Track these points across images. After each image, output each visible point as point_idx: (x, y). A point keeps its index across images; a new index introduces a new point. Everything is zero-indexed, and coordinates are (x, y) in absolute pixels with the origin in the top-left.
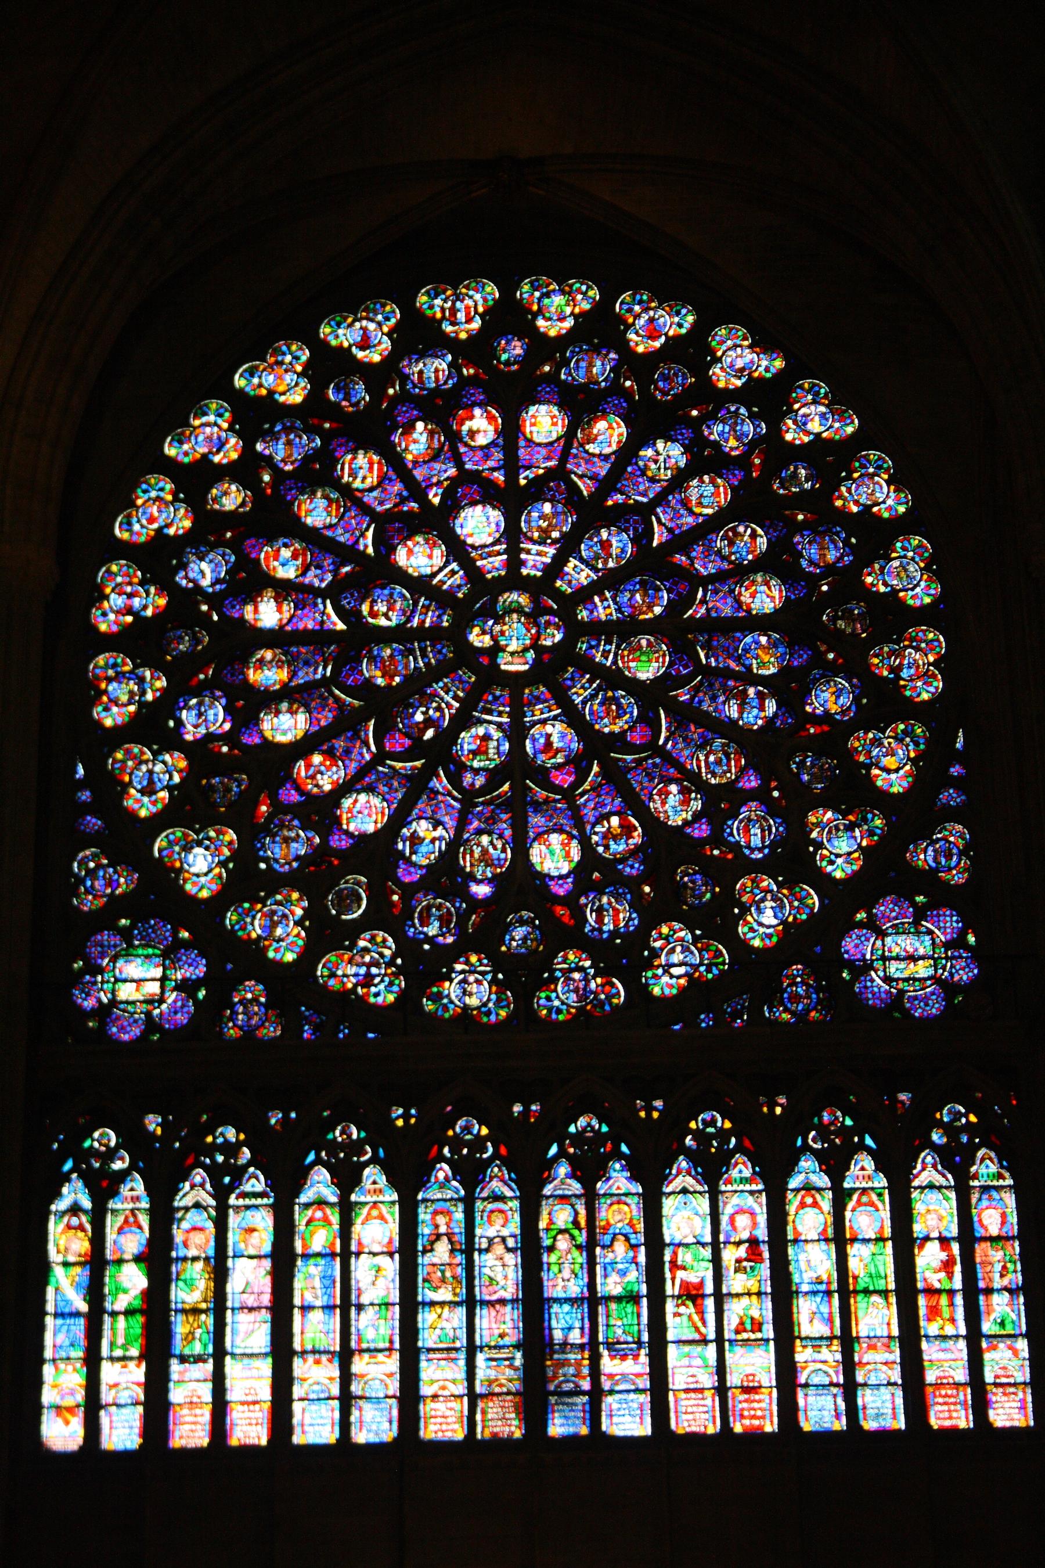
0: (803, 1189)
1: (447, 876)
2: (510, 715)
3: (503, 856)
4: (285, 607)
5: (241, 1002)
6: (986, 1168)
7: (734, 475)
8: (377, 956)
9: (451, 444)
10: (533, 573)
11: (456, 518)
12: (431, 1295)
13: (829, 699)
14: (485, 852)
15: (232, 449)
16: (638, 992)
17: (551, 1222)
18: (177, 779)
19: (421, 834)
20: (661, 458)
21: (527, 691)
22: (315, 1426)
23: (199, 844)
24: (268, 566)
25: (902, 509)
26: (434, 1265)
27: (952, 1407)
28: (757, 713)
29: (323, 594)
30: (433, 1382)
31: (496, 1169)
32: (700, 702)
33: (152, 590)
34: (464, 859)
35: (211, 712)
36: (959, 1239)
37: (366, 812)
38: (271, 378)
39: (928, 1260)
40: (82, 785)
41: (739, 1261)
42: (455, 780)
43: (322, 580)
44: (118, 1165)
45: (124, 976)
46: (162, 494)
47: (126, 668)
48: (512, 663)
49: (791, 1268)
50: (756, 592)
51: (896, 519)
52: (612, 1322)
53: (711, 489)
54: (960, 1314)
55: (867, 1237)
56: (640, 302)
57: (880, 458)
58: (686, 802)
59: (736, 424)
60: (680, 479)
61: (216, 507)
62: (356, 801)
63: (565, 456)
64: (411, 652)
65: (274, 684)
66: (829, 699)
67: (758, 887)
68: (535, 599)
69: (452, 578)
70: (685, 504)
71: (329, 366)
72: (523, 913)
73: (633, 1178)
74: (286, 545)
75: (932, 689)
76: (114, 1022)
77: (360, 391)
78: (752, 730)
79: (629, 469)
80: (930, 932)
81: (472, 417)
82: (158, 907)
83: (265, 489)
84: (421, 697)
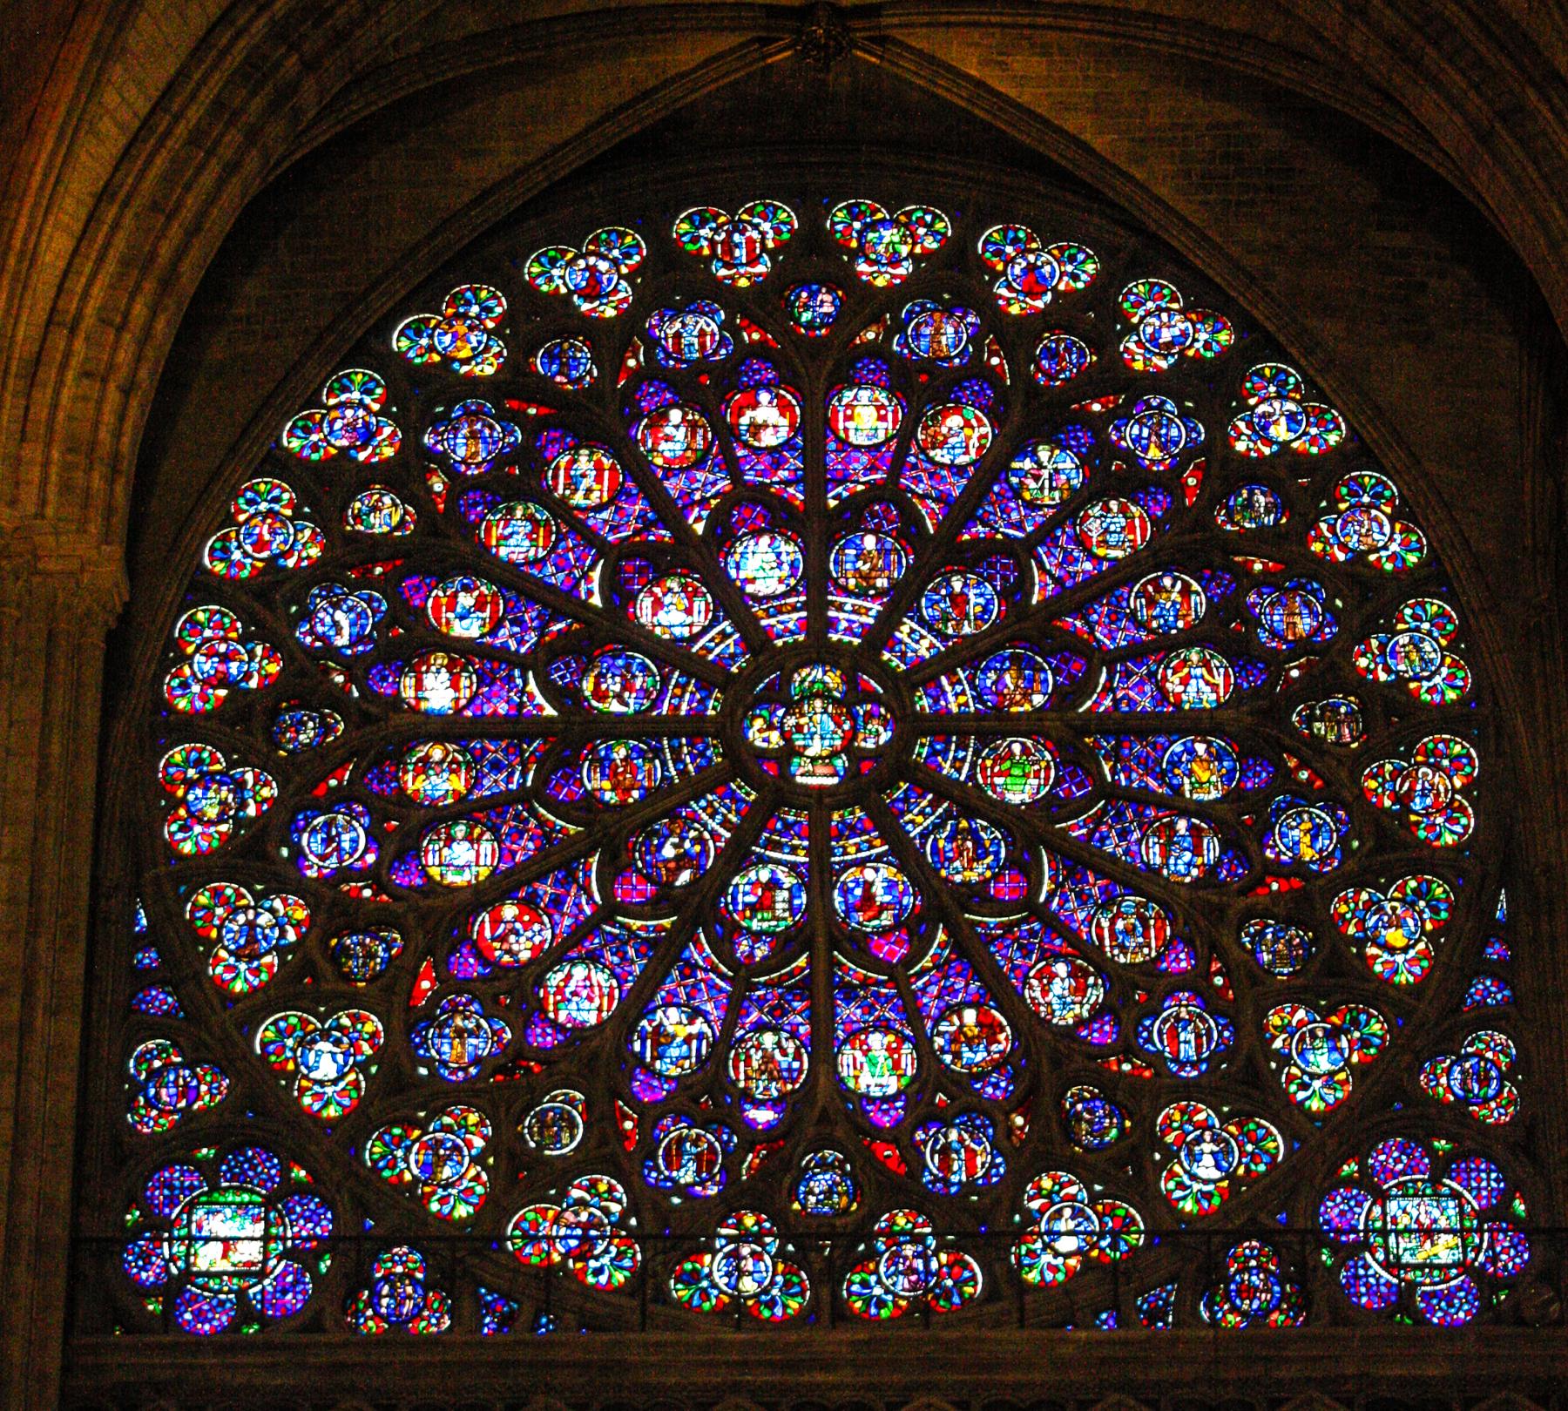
1: (710, 1093)
3: (796, 1065)
4: (464, 682)
5: (387, 1279)
7: (1157, 502)
8: (598, 1213)
9: (725, 444)
10: (846, 639)
11: (729, 554)
13: (1302, 839)
14: (768, 1059)
18: (291, 936)
19: (670, 1029)
20: (1045, 473)
21: (836, 817)
23: (325, 1035)
24: (438, 619)
25: (1412, 558)
29: (524, 663)
32: (1103, 839)
33: (259, 650)
34: (736, 1068)
35: (345, 837)
37: (584, 993)
38: (447, 339)
43: (521, 642)
45: (204, 1233)
46: (277, 507)
47: (217, 767)
48: (813, 774)
51: (1402, 570)
56: (1015, 241)
57: (1379, 482)
58: (1080, 990)
59: (1160, 425)
60: (1072, 508)
61: (359, 527)
62: (569, 977)
63: (898, 465)
65: (445, 797)
66: (1302, 839)
67: (1190, 1121)
68: (849, 679)
69: (723, 643)
70: (1082, 541)
71: (536, 321)
72: (827, 1152)
74: (467, 589)
75: (1458, 829)
76: (189, 1303)
77: (586, 366)
78: (1183, 884)
79: (996, 489)
80: (1455, 1195)
81: (755, 405)
82: (259, 1129)
83: (437, 504)
84: (672, 822)
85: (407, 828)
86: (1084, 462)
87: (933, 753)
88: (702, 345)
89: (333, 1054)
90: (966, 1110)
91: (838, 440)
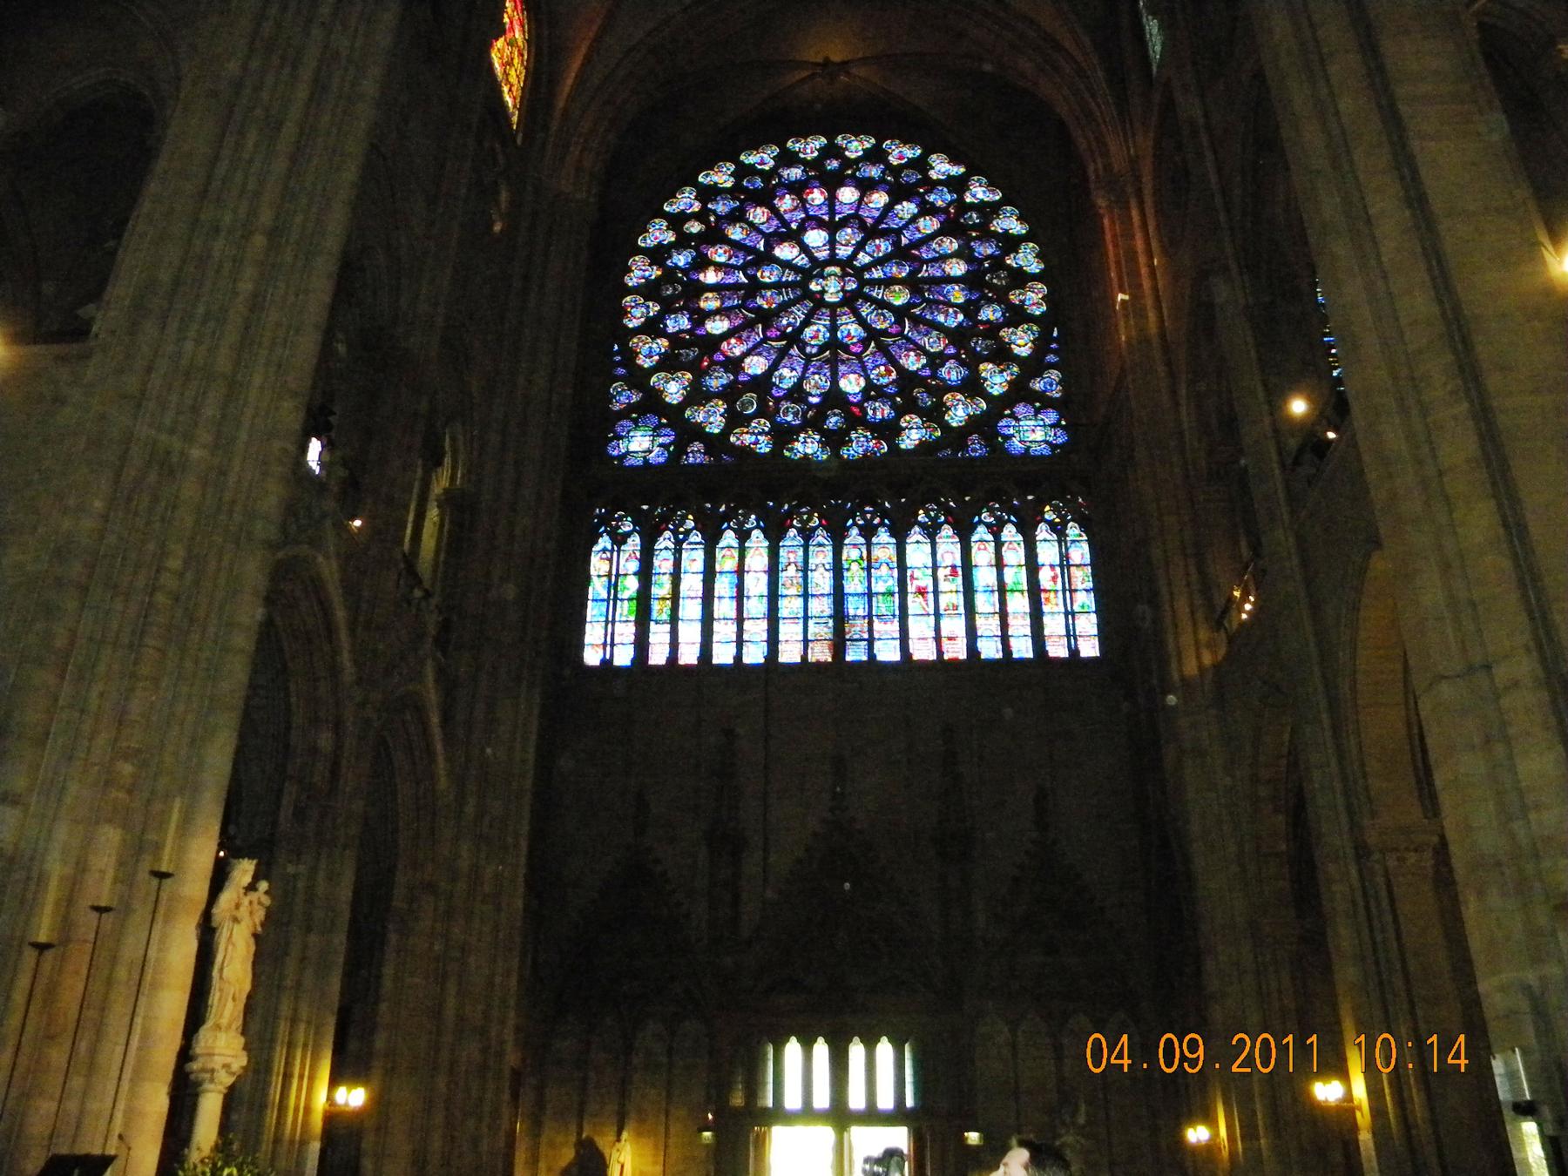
9: (803, 204)
13: (989, 313)
15: (697, 207)
16: (894, 448)
22: (723, 655)
28: (954, 320)
36: (1061, 566)
39: (1045, 577)
40: (618, 353)
42: (802, 350)
44: (627, 529)
60: (914, 219)
63: (858, 208)
66: (989, 313)
68: (843, 269)
70: (918, 229)
71: (743, 171)
73: (892, 536)
77: (759, 183)
85: (700, 317)
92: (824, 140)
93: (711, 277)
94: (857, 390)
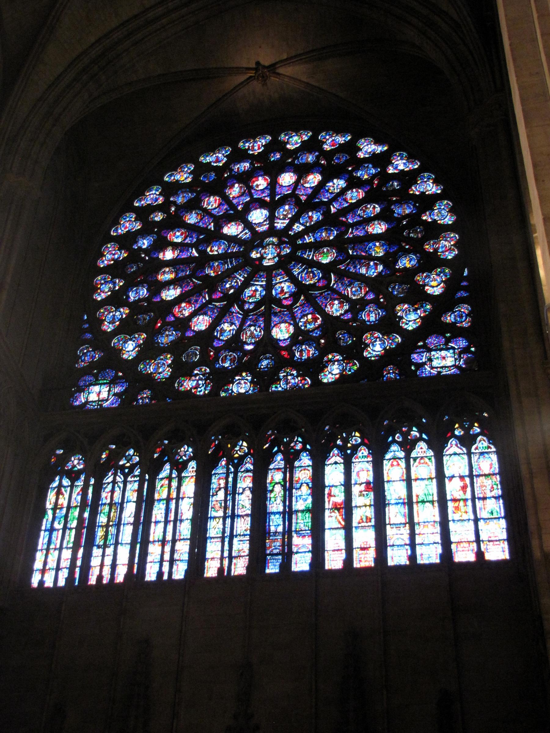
0: (392, 459)
2: (266, 281)
3: (260, 334)
4: (176, 252)
5: (141, 398)
6: (482, 443)
9: (249, 189)
11: (248, 215)
12: (214, 514)
13: (406, 263)
14: (252, 333)
15: (161, 200)
16: (317, 382)
17: (272, 479)
18: (124, 316)
19: (225, 329)
20: (335, 186)
23: (131, 340)
26: (217, 501)
27: (467, 552)
28: (373, 271)
30: (212, 552)
31: (249, 459)
32: (349, 269)
34: (243, 336)
38: (179, 176)
41: (361, 492)
42: (241, 307)
49: (386, 493)
50: (374, 227)
52: (299, 521)
53: (356, 194)
54: (470, 509)
55: (423, 478)
56: (329, 135)
57: (429, 175)
58: (342, 307)
59: (367, 170)
60: (343, 191)
62: (198, 318)
64: (226, 263)
66: (406, 263)
68: (280, 240)
70: (346, 200)
74: (178, 231)
77: (213, 175)
81: (258, 180)
85: (157, 287)
86: (346, 181)
87: (302, 254)
88: (245, 169)
89: (132, 344)
90: (307, 340)
91: (279, 185)
92: (269, 138)
93: (169, 255)
94: (287, 336)
